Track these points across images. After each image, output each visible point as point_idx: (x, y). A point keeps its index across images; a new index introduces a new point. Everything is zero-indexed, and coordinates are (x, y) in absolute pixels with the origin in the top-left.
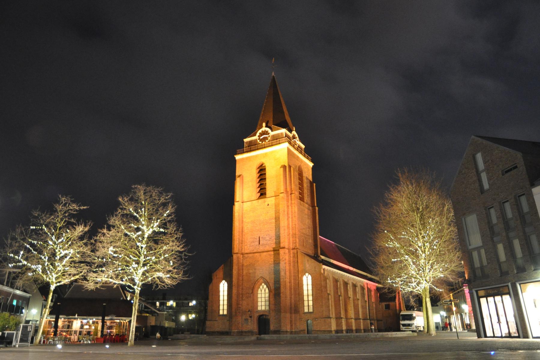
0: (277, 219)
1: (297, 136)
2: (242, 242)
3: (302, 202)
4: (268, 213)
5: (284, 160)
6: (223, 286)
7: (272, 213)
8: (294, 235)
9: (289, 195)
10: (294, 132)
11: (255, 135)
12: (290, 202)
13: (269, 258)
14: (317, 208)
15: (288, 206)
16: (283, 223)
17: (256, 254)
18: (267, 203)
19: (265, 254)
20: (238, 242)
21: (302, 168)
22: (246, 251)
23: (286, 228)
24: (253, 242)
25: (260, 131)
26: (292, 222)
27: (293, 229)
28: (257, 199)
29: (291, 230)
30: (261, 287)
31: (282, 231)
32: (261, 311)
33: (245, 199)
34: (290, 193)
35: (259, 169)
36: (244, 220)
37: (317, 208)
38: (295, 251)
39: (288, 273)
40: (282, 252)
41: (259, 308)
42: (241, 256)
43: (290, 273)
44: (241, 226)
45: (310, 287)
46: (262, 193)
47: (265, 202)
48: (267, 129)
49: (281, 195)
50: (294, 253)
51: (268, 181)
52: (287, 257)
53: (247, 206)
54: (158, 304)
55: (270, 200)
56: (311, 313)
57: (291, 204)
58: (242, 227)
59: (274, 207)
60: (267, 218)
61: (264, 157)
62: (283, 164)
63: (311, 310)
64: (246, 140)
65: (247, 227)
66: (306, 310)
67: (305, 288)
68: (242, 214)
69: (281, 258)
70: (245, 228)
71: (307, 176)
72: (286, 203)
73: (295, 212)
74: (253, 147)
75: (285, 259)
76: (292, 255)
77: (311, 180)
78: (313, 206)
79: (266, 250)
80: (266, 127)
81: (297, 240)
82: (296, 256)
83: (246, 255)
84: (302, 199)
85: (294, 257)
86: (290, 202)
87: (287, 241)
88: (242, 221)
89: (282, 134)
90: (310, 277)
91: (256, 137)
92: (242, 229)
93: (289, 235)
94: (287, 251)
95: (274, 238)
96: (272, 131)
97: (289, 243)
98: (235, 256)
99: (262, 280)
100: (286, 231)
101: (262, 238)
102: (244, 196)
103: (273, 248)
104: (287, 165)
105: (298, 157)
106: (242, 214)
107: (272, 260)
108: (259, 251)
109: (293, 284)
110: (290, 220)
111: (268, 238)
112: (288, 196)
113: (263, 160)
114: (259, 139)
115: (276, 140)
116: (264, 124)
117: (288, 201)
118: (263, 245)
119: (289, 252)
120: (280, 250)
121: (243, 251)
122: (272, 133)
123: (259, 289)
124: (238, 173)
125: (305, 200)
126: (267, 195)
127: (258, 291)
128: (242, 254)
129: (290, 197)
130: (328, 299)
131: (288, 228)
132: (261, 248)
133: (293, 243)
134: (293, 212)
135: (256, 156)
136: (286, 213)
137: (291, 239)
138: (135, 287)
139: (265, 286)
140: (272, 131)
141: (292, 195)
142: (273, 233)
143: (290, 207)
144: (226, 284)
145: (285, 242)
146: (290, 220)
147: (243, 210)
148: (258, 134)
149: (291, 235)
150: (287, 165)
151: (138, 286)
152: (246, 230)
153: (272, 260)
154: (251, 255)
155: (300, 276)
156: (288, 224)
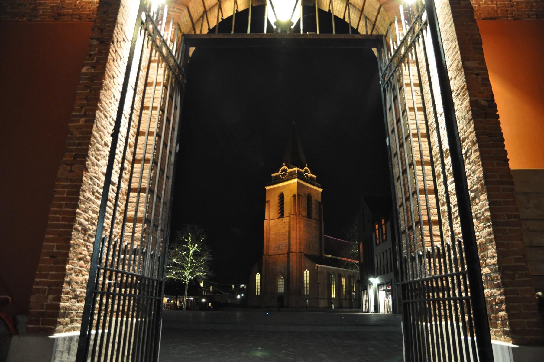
0: (289, 232)
1: (309, 170)
2: (268, 248)
3: (309, 219)
4: (284, 228)
5: (295, 191)
6: (258, 277)
7: (287, 228)
8: (300, 243)
9: (298, 215)
10: (306, 168)
11: (279, 172)
12: (298, 220)
13: (283, 258)
14: (323, 222)
15: (296, 224)
16: (293, 235)
17: (277, 256)
18: (284, 221)
19: (282, 256)
20: (265, 248)
21: (312, 194)
22: (272, 254)
23: (295, 239)
24: (276, 247)
25: (281, 169)
26: (299, 235)
27: (299, 239)
28: (278, 218)
29: (298, 240)
30: (280, 278)
31: (292, 241)
32: (280, 293)
33: (271, 218)
34: (298, 214)
35: (280, 197)
36: (270, 232)
37: (323, 222)
38: (300, 254)
39: (295, 269)
40: (291, 254)
41: (279, 291)
42: (268, 257)
43: (296, 269)
44: (268, 237)
45: (308, 279)
46: (282, 214)
47: (283, 220)
48: (286, 167)
49: (292, 216)
50: (299, 256)
51: (285, 205)
52: (294, 259)
53: (272, 222)
54: (233, 286)
55: (286, 219)
56: (308, 295)
57: (299, 222)
58: (269, 237)
59: (288, 224)
60: (284, 232)
61: (283, 188)
62: (294, 193)
63: (308, 293)
64: (273, 175)
65: (272, 237)
66: (305, 293)
67: (305, 278)
68: (269, 228)
69: (290, 259)
70: (271, 238)
71: (317, 199)
72: (295, 221)
73: (301, 228)
74: (278, 180)
75: (293, 260)
76: (298, 257)
77: (320, 201)
78: (320, 221)
79: (283, 253)
80: (285, 166)
81: (302, 247)
82: (300, 258)
83: (271, 256)
84: (309, 216)
85: (299, 258)
86: (298, 220)
87: (295, 247)
88: (269, 233)
89: (295, 171)
90: (308, 272)
91: (279, 173)
92: (269, 239)
93: (296, 243)
94: (294, 254)
95: (287, 245)
96: (289, 169)
97: (296, 248)
98: (264, 257)
99: (280, 273)
100: (295, 241)
101: (281, 245)
102: (270, 215)
103: (287, 252)
104: (296, 194)
105: (308, 187)
106: (269, 228)
107: (286, 260)
108: (279, 253)
109: (298, 276)
110: (298, 233)
111: (284, 245)
112: (296, 217)
113: (283, 191)
114: (281, 175)
115: (291, 176)
116: (284, 164)
117: (296, 220)
118: (281, 249)
119: (296, 255)
120: (290, 253)
121: (269, 254)
122: (289, 171)
123: (279, 279)
124: (267, 200)
125: (313, 217)
126: (285, 216)
127: (278, 280)
128: (269, 255)
129: (298, 218)
130: (318, 287)
131: (296, 239)
132: (280, 252)
133: (299, 249)
134: (300, 227)
135: (278, 187)
136: (295, 228)
137: (298, 246)
138: (186, 280)
139: (282, 277)
140: (289, 169)
141: (300, 216)
142: (287, 242)
143: (298, 224)
144: (259, 275)
145: (294, 248)
146: (298, 233)
147: (269, 226)
148: (280, 171)
149: (298, 243)
150: (296, 194)
151: (187, 280)
152: (271, 240)
153: (286, 260)
154: (274, 256)
155: (302, 271)
156: (296, 236)
